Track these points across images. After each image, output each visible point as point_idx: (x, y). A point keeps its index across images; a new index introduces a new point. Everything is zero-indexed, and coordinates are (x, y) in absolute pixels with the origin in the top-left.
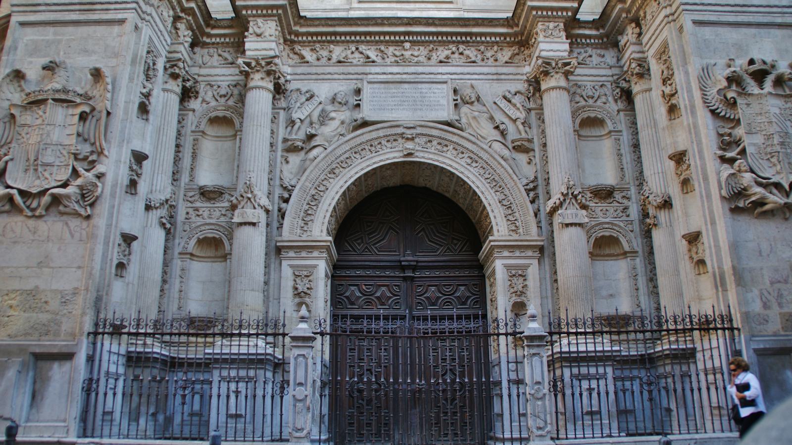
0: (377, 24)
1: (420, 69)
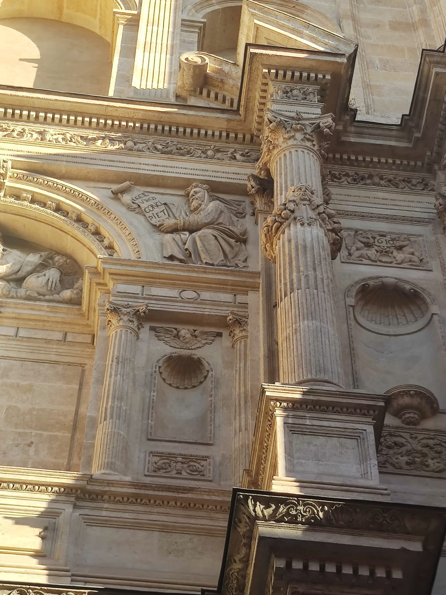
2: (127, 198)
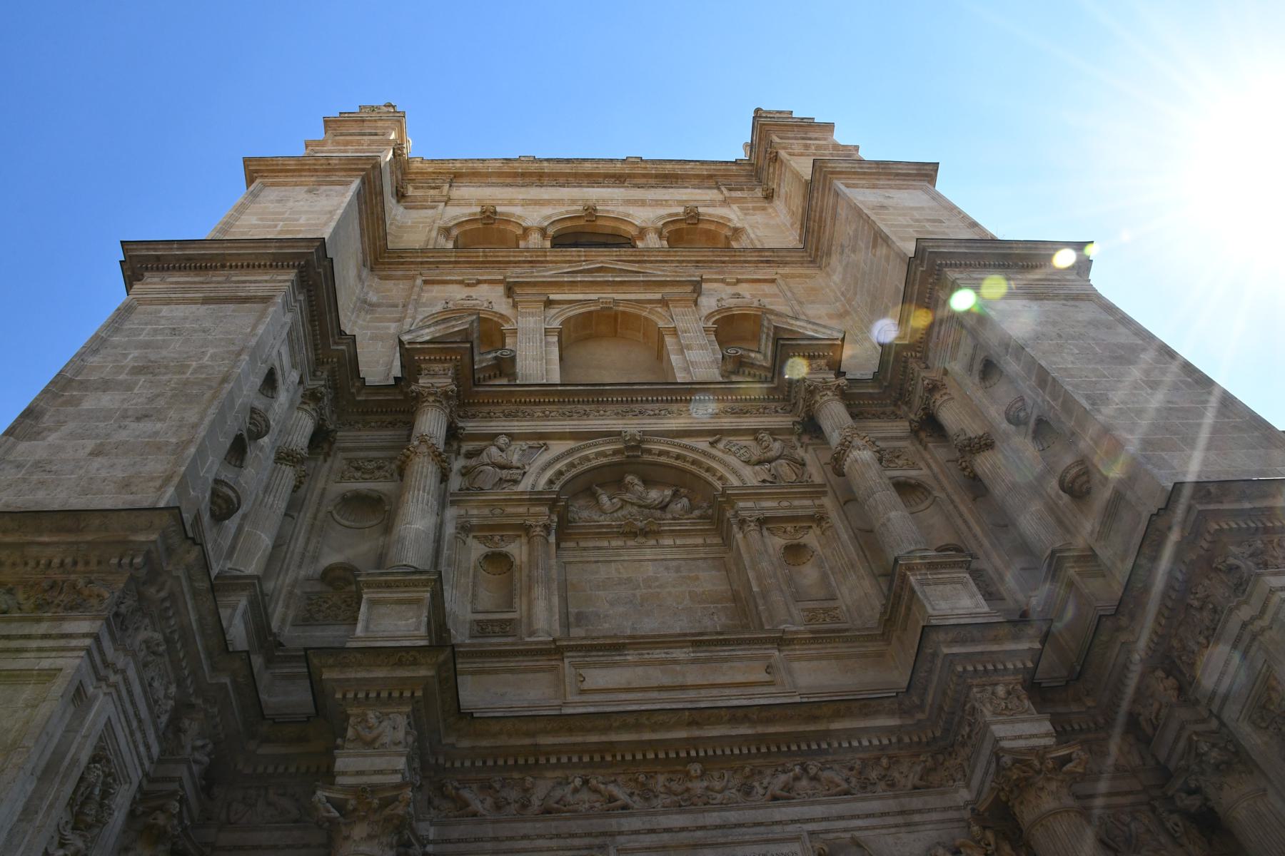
0: (625, 727)
1: (733, 816)
2: (721, 445)
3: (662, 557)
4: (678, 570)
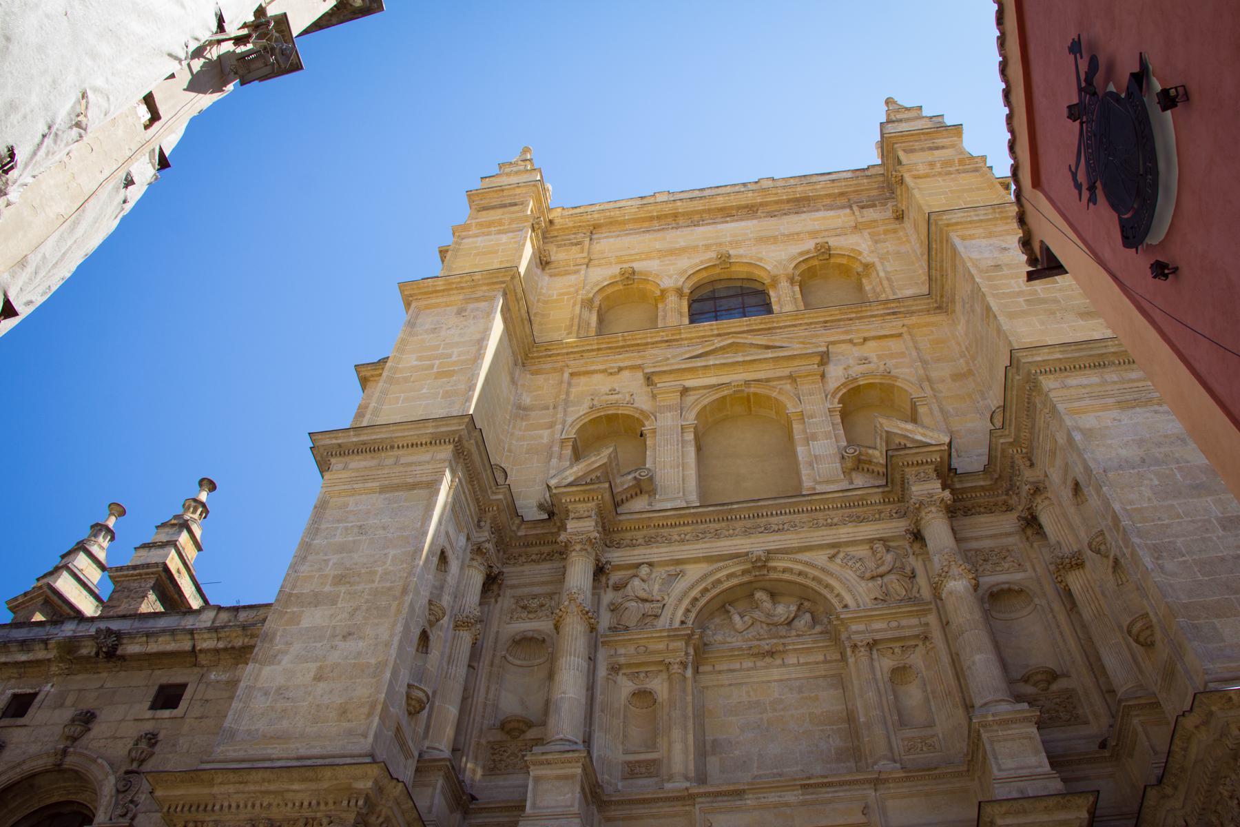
3: (787, 677)
4: (800, 691)
